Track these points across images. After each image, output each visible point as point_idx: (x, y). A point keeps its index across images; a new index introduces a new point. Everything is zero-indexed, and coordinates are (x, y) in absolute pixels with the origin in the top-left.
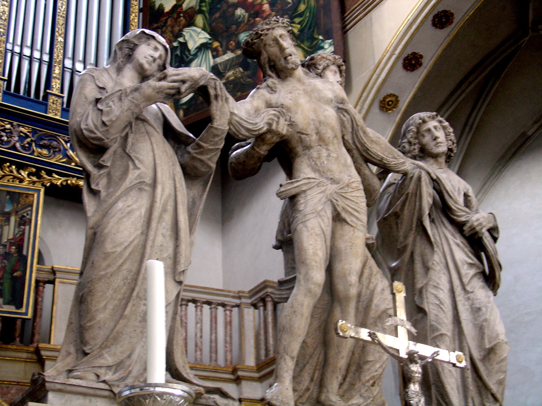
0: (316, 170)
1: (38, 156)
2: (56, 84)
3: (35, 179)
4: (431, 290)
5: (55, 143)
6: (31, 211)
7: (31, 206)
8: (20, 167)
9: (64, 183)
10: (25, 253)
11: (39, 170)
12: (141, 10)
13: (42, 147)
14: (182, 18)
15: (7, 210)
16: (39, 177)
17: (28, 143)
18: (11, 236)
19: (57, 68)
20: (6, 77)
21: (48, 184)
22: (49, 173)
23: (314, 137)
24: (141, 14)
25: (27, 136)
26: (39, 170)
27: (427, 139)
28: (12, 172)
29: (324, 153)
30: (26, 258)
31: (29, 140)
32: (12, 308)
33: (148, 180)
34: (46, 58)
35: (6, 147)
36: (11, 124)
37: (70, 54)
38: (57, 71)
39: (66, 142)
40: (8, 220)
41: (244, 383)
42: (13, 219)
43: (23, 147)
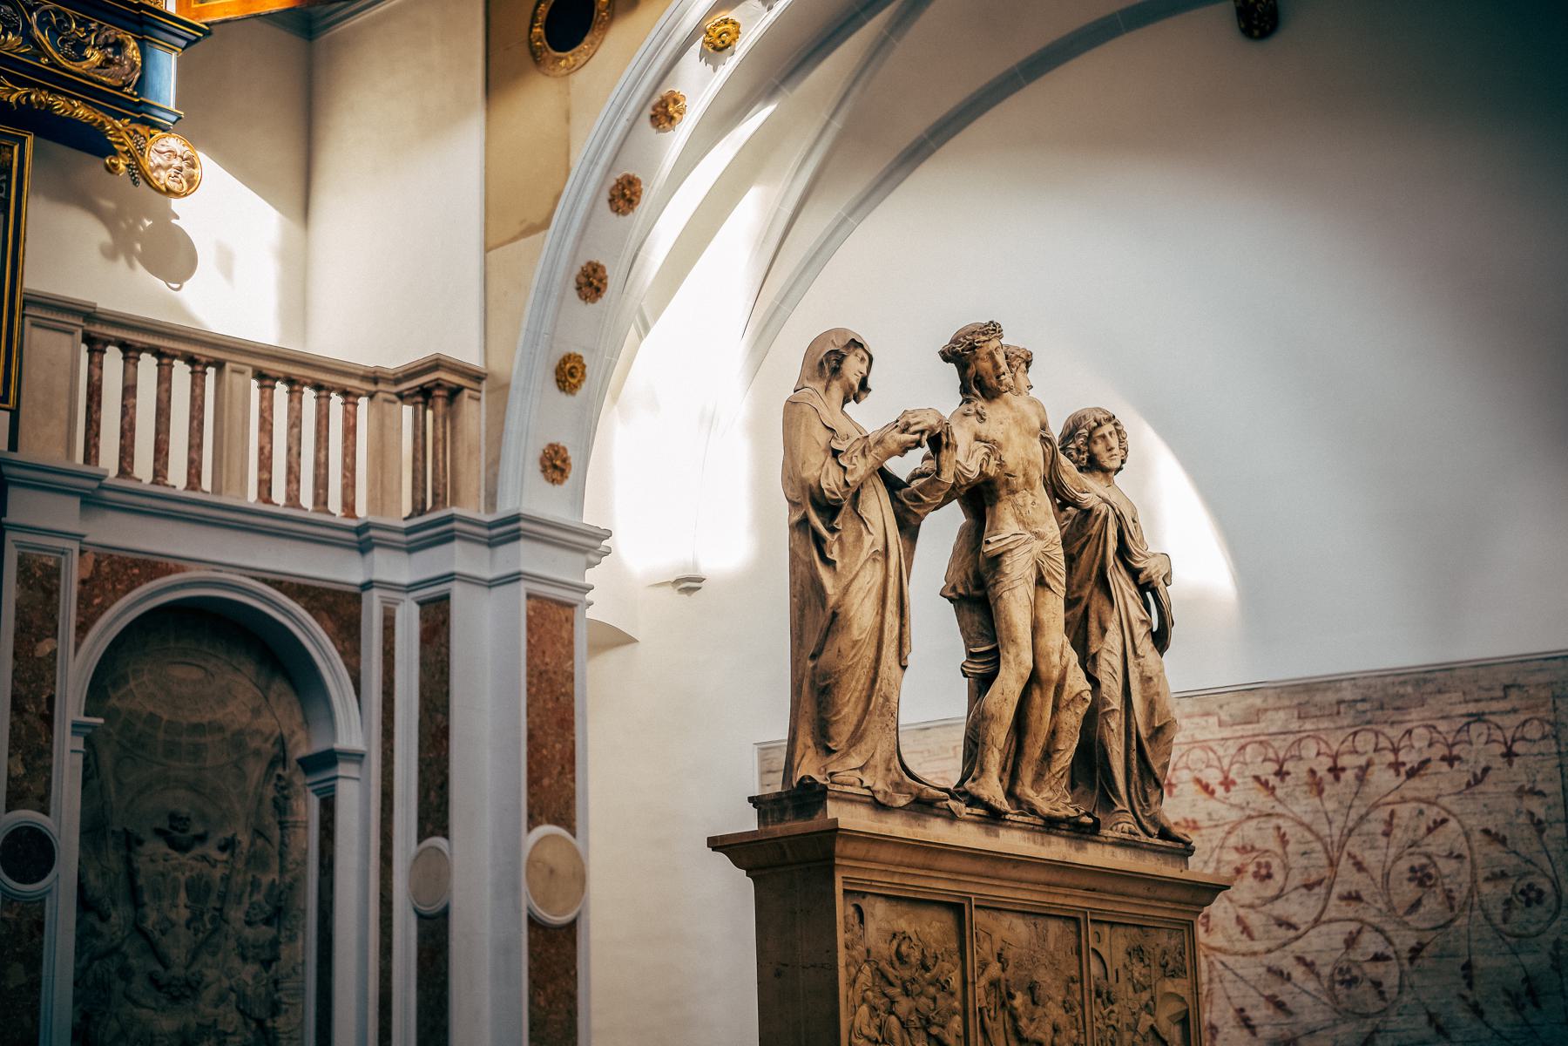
0: (1021, 521)
4: (1104, 655)
23: (1021, 480)
27: (1099, 448)
29: (1029, 499)
33: (880, 547)
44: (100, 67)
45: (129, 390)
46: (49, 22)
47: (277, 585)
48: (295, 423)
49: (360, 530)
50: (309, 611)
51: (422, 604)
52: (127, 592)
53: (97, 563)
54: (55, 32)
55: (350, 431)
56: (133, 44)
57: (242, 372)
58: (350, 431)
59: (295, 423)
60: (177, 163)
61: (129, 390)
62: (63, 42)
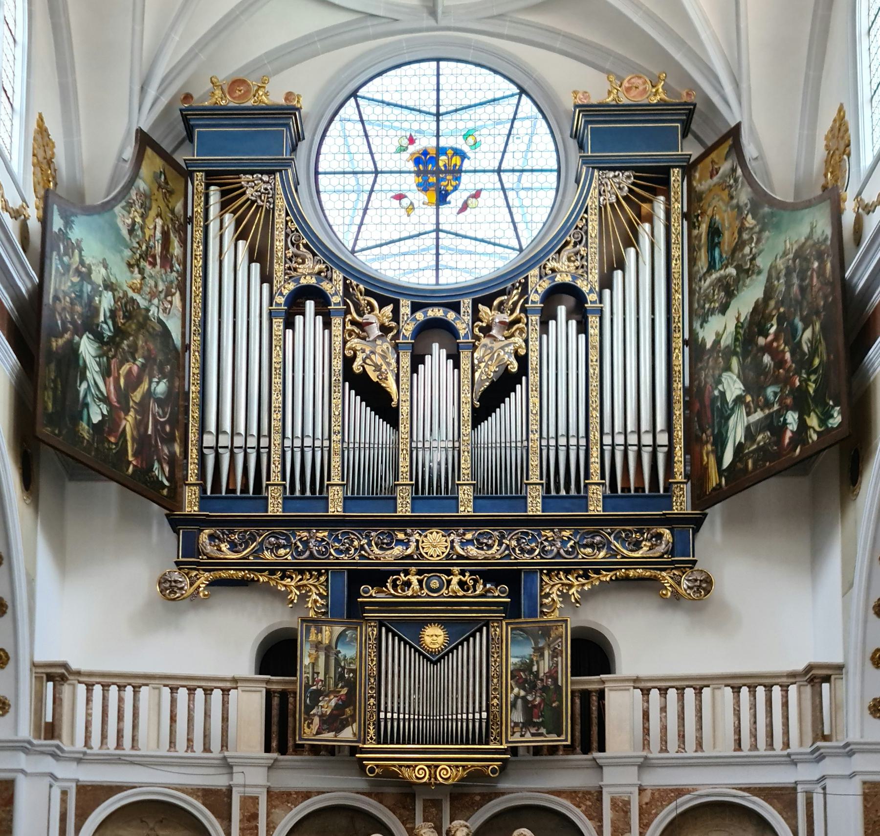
1: (583, 558)
2: (595, 467)
3: (583, 581)
5: (598, 538)
6: (561, 642)
7: (561, 637)
8: (567, 572)
9: (613, 578)
10: (560, 684)
11: (586, 571)
12: (685, 342)
13: (586, 546)
14: (721, 359)
15: (540, 645)
16: (587, 577)
17: (571, 547)
18: (547, 670)
19: (595, 449)
20: (544, 481)
21: (597, 583)
22: (597, 572)
24: (687, 349)
25: (570, 539)
26: (586, 571)
28: (561, 579)
30: (560, 688)
31: (572, 543)
32: (554, 737)
34: (583, 442)
35: (550, 557)
36: (552, 530)
37: (607, 429)
38: (595, 453)
39: (610, 534)
40: (542, 655)
41: (799, 765)
42: (546, 653)
43: (567, 552)
44: (650, 549)
45: (664, 709)
46: (621, 537)
47: (747, 789)
48: (753, 706)
49: (789, 755)
50: (766, 801)
51: (864, 783)
52: (667, 805)
53: (653, 794)
54: (623, 541)
55: (785, 704)
56: (668, 531)
57: (719, 688)
58: (785, 704)
59: (753, 706)
60: (698, 583)
61: (664, 709)
62: (629, 544)
